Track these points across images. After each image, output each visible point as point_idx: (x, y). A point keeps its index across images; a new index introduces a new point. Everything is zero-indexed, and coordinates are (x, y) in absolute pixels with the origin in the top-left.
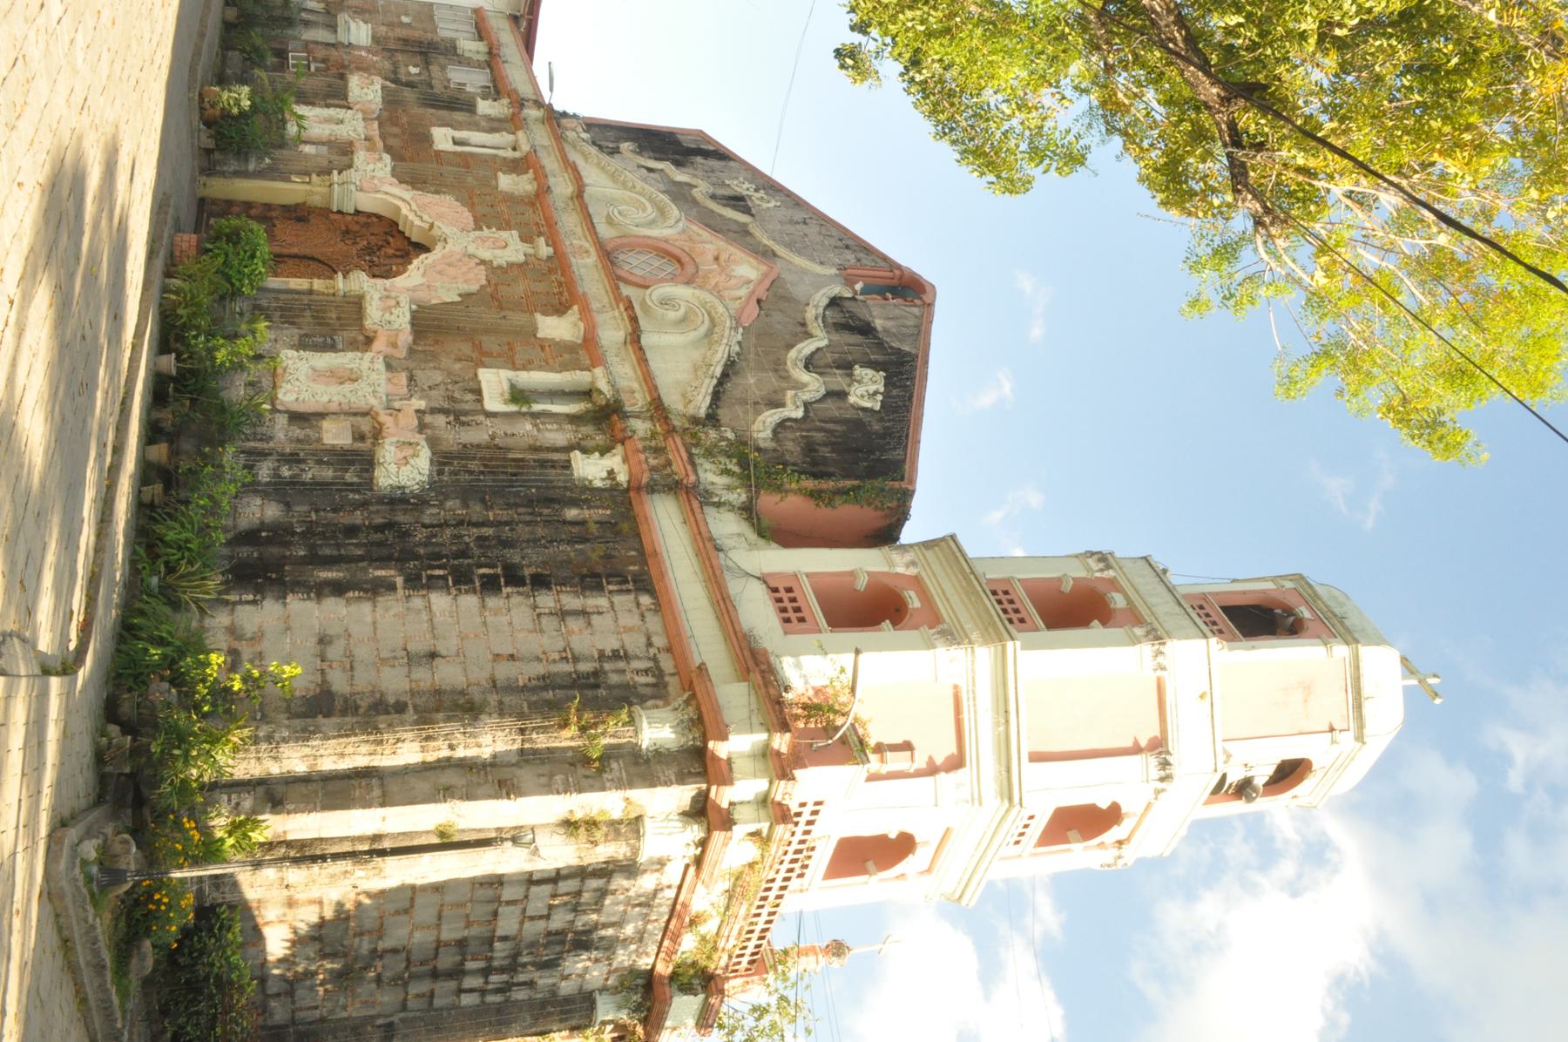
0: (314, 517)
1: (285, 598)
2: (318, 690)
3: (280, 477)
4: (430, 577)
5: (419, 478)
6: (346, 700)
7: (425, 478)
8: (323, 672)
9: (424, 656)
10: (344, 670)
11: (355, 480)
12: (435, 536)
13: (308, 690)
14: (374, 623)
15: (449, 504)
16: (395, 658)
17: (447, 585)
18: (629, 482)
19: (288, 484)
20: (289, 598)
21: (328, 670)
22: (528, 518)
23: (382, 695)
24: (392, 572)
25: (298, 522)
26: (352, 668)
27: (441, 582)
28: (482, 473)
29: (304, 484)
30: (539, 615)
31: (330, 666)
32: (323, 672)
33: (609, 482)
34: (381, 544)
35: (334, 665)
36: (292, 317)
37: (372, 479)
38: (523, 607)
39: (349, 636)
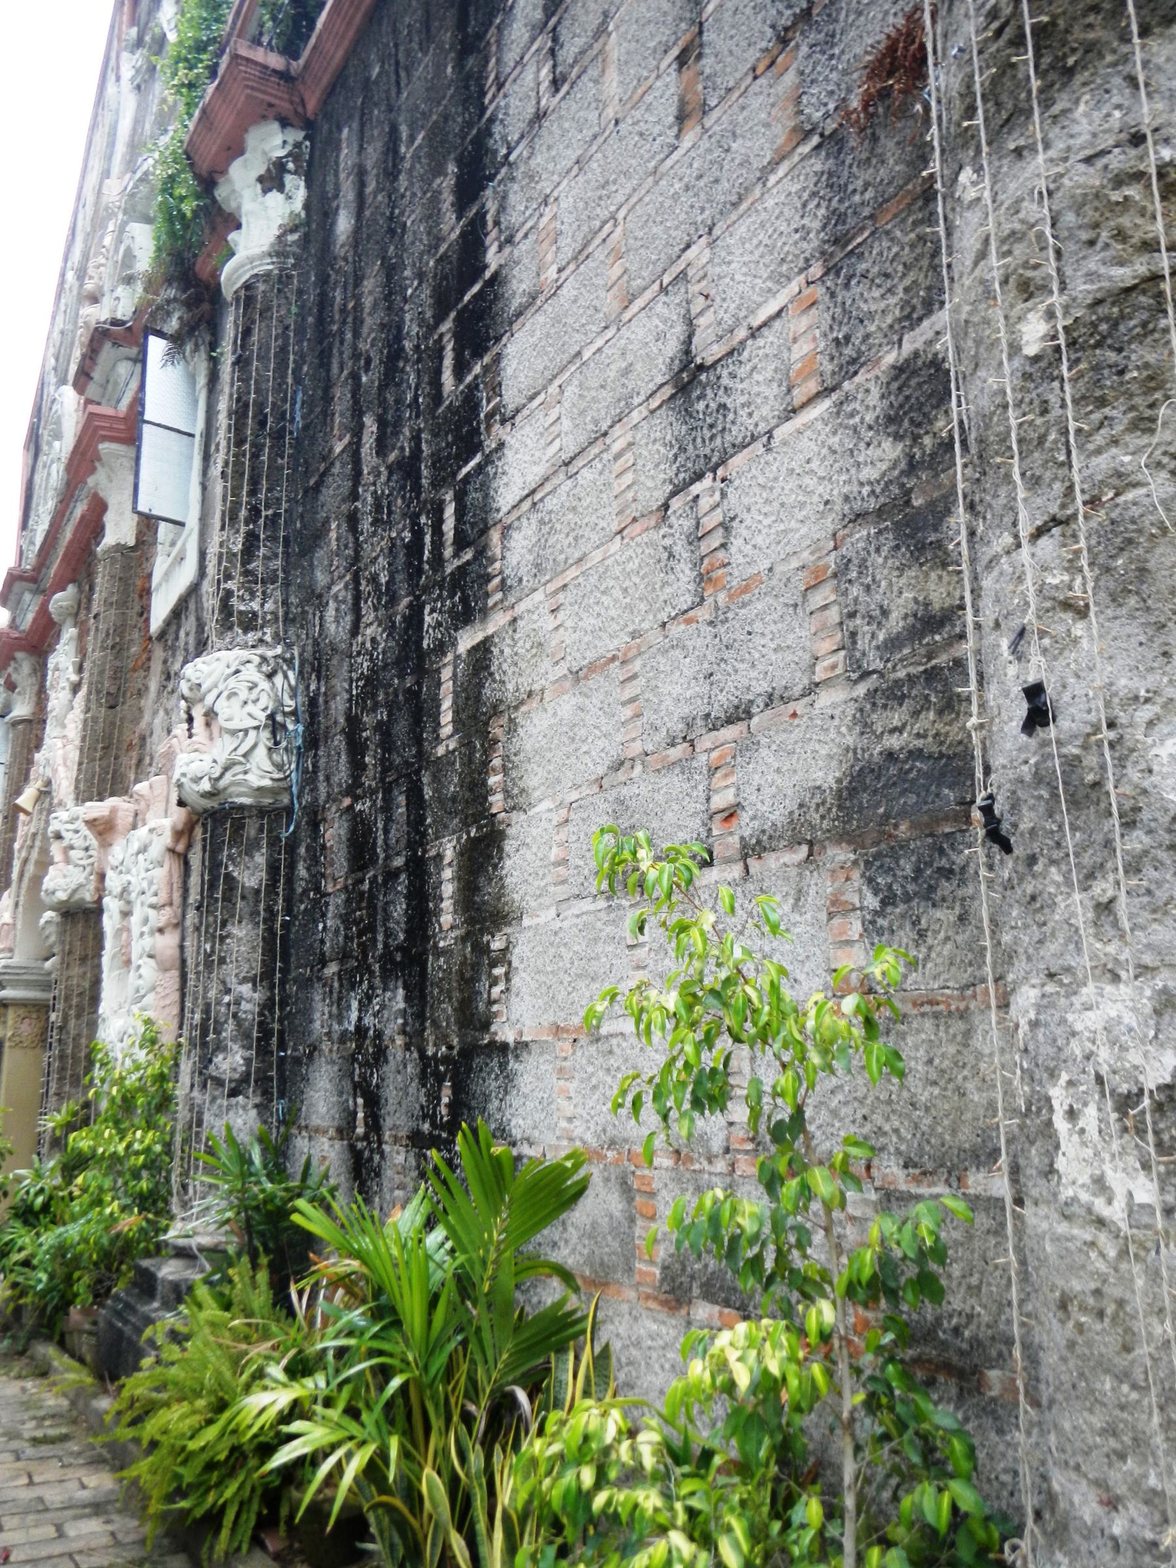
0: (332, 969)
1: (504, 1047)
2: (840, 854)
3: (245, 1079)
4: (461, 542)
5: (251, 673)
6: (893, 694)
7: (253, 656)
8: (752, 850)
9: (688, 413)
10: (747, 747)
11: (260, 859)
12: (374, 579)
13: (837, 908)
14: (576, 675)
15: (321, 578)
16: (696, 538)
17: (480, 468)
18: (285, 123)
19: (263, 1050)
20: (505, 1033)
21: (746, 826)
22: (349, 336)
23: (859, 517)
24: (446, 674)
25: (340, 1023)
26: (739, 714)
27: (474, 496)
28: (255, 512)
29: (267, 1006)
30: (556, 84)
31: (730, 814)
32: (752, 850)
33: (289, 180)
34: (387, 743)
35: (720, 801)
36: (76, 1060)
37: (262, 812)
38: (538, 160)
39: (618, 765)
